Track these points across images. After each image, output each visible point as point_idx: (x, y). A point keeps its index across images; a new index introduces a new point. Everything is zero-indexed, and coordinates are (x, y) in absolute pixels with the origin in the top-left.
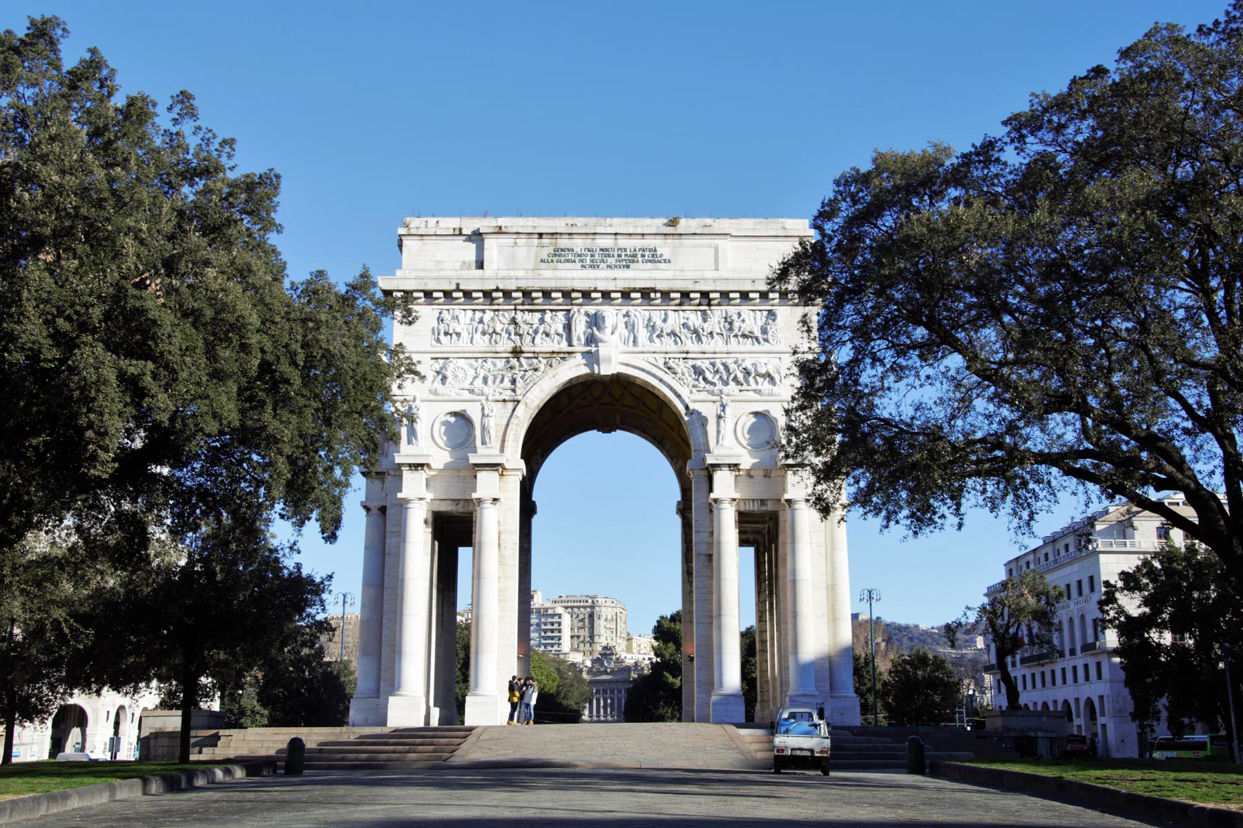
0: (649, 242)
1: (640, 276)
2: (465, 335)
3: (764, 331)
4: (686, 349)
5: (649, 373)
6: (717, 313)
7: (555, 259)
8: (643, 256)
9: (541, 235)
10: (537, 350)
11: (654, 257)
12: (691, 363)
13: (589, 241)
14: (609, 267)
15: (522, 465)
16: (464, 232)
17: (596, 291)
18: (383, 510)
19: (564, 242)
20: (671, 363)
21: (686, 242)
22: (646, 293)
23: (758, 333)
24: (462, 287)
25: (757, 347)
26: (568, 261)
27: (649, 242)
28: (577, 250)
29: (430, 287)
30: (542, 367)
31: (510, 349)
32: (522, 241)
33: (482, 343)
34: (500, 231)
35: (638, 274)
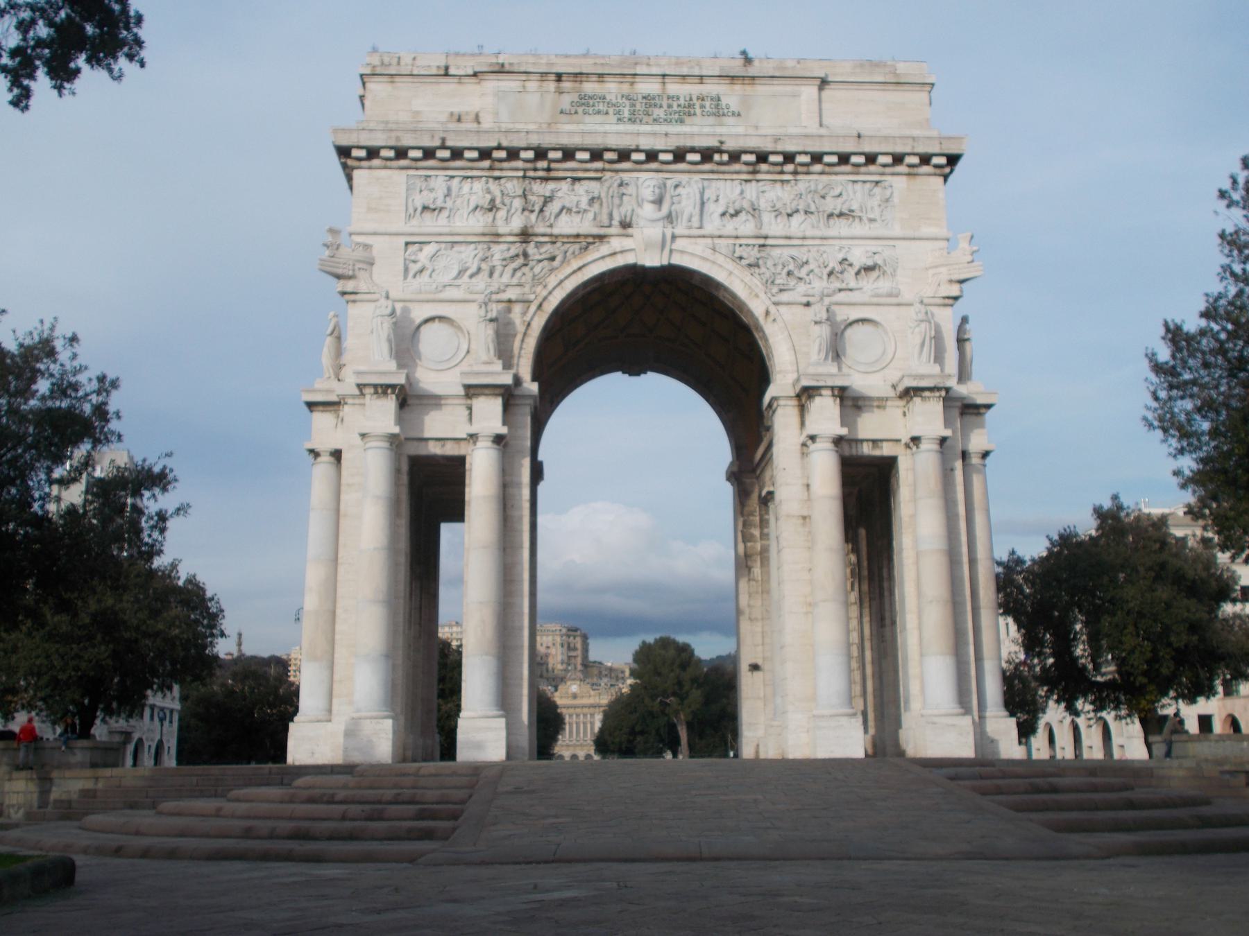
0: (711, 88)
1: (699, 132)
7: (580, 110)
8: (702, 107)
9: (559, 77)
10: (556, 231)
11: (719, 111)
15: (534, 388)
16: (452, 71)
17: (637, 150)
18: (337, 455)
19: (590, 87)
21: (761, 89)
22: (707, 155)
24: (449, 143)
26: (599, 112)
27: (711, 88)
32: (532, 85)
33: (479, 223)
35: (695, 129)
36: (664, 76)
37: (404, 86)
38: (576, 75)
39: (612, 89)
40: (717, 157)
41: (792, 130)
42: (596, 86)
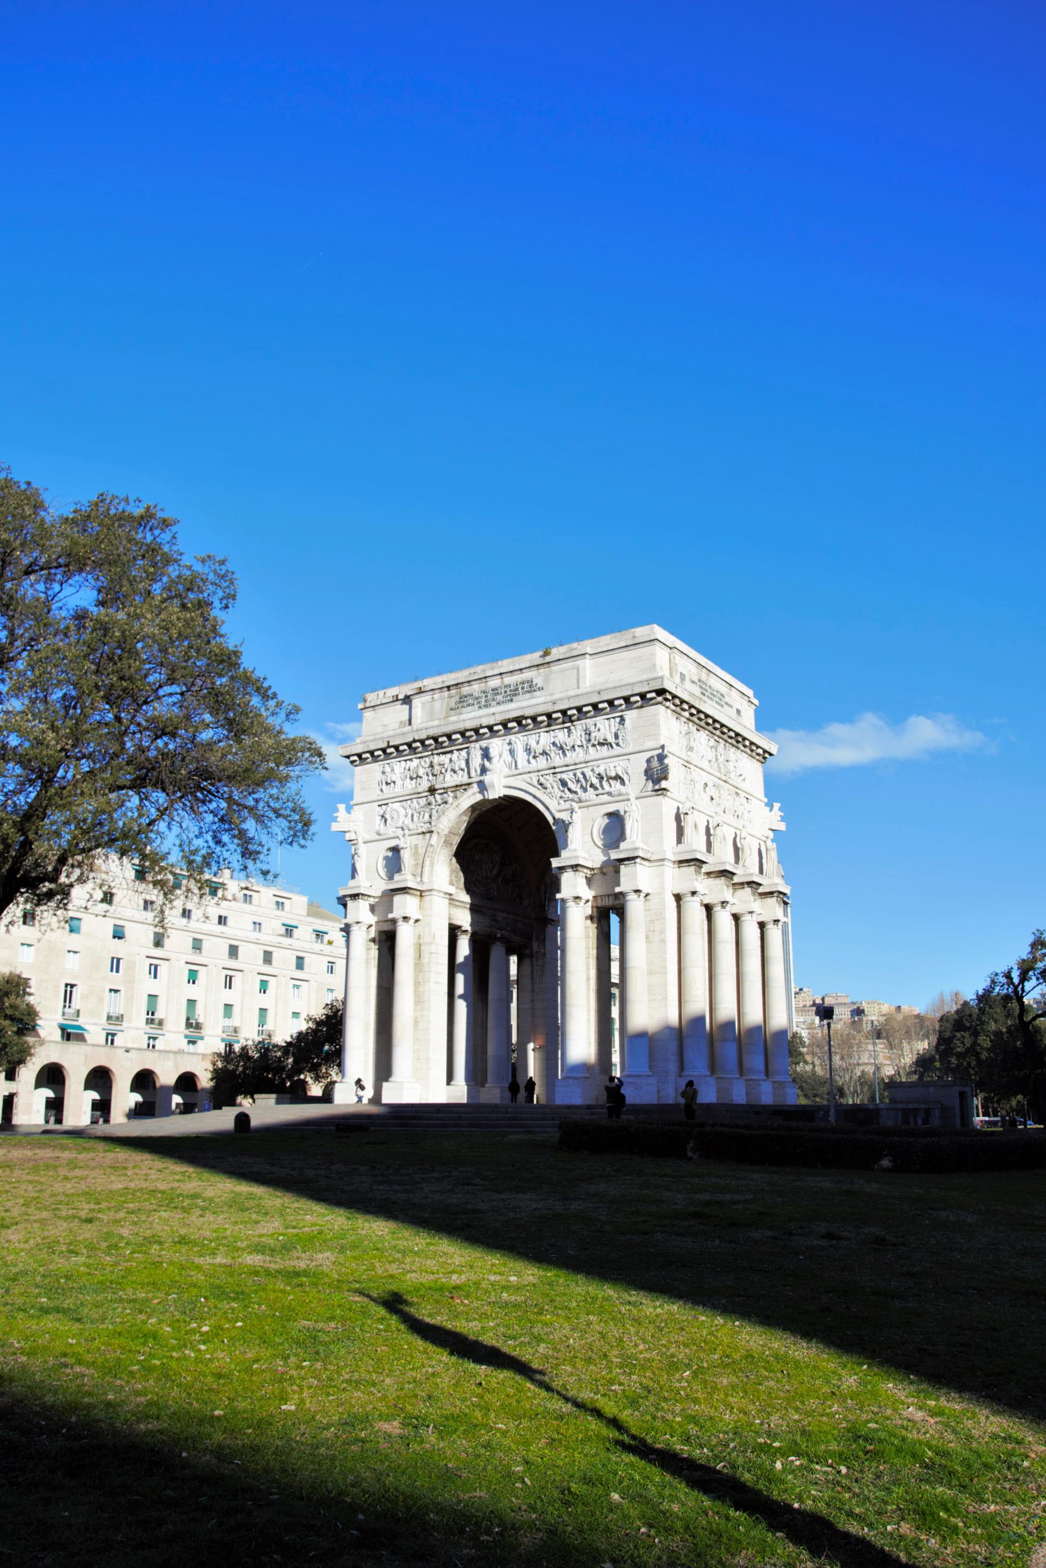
2: (399, 783)
3: (616, 736)
4: (552, 765)
5: (526, 792)
6: (579, 727)
9: (448, 688)
10: (445, 785)
11: (531, 688)
12: (559, 776)
13: (483, 685)
14: (498, 703)
19: (466, 690)
20: (542, 780)
21: (555, 668)
22: (518, 720)
23: (611, 739)
25: (612, 752)
27: (526, 675)
28: (476, 694)
29: (372, 747)
30: (450, 800)
31: (427, 789)
32: (437, 696)
33: (410, 786)
34: (420, 691)
36: (501, 674)
37: (380, 711)
38: (457, 685)
39: (476, 688)
40: (524, 722)
41: (572, 693)
42: (467, 688)
